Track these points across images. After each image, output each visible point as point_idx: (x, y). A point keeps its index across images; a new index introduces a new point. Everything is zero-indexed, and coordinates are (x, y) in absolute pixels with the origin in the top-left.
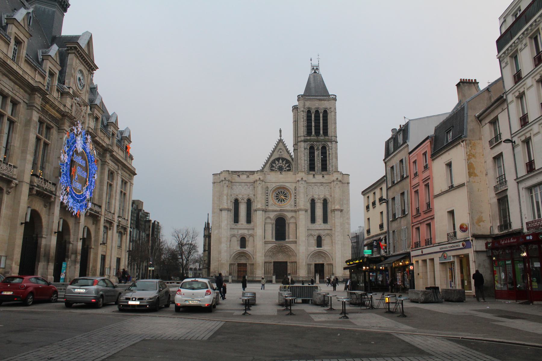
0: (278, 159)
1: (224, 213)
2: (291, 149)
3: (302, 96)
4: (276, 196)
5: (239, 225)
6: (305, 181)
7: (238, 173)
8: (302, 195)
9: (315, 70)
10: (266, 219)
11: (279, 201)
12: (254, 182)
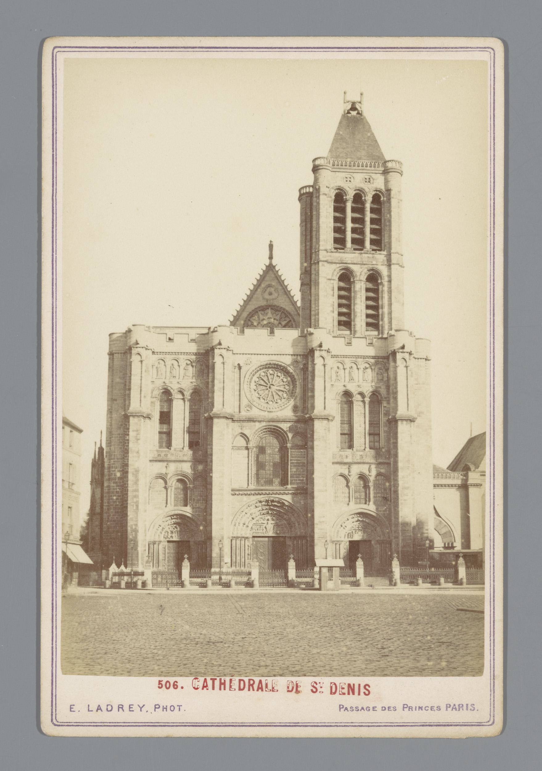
0: (263, 309)
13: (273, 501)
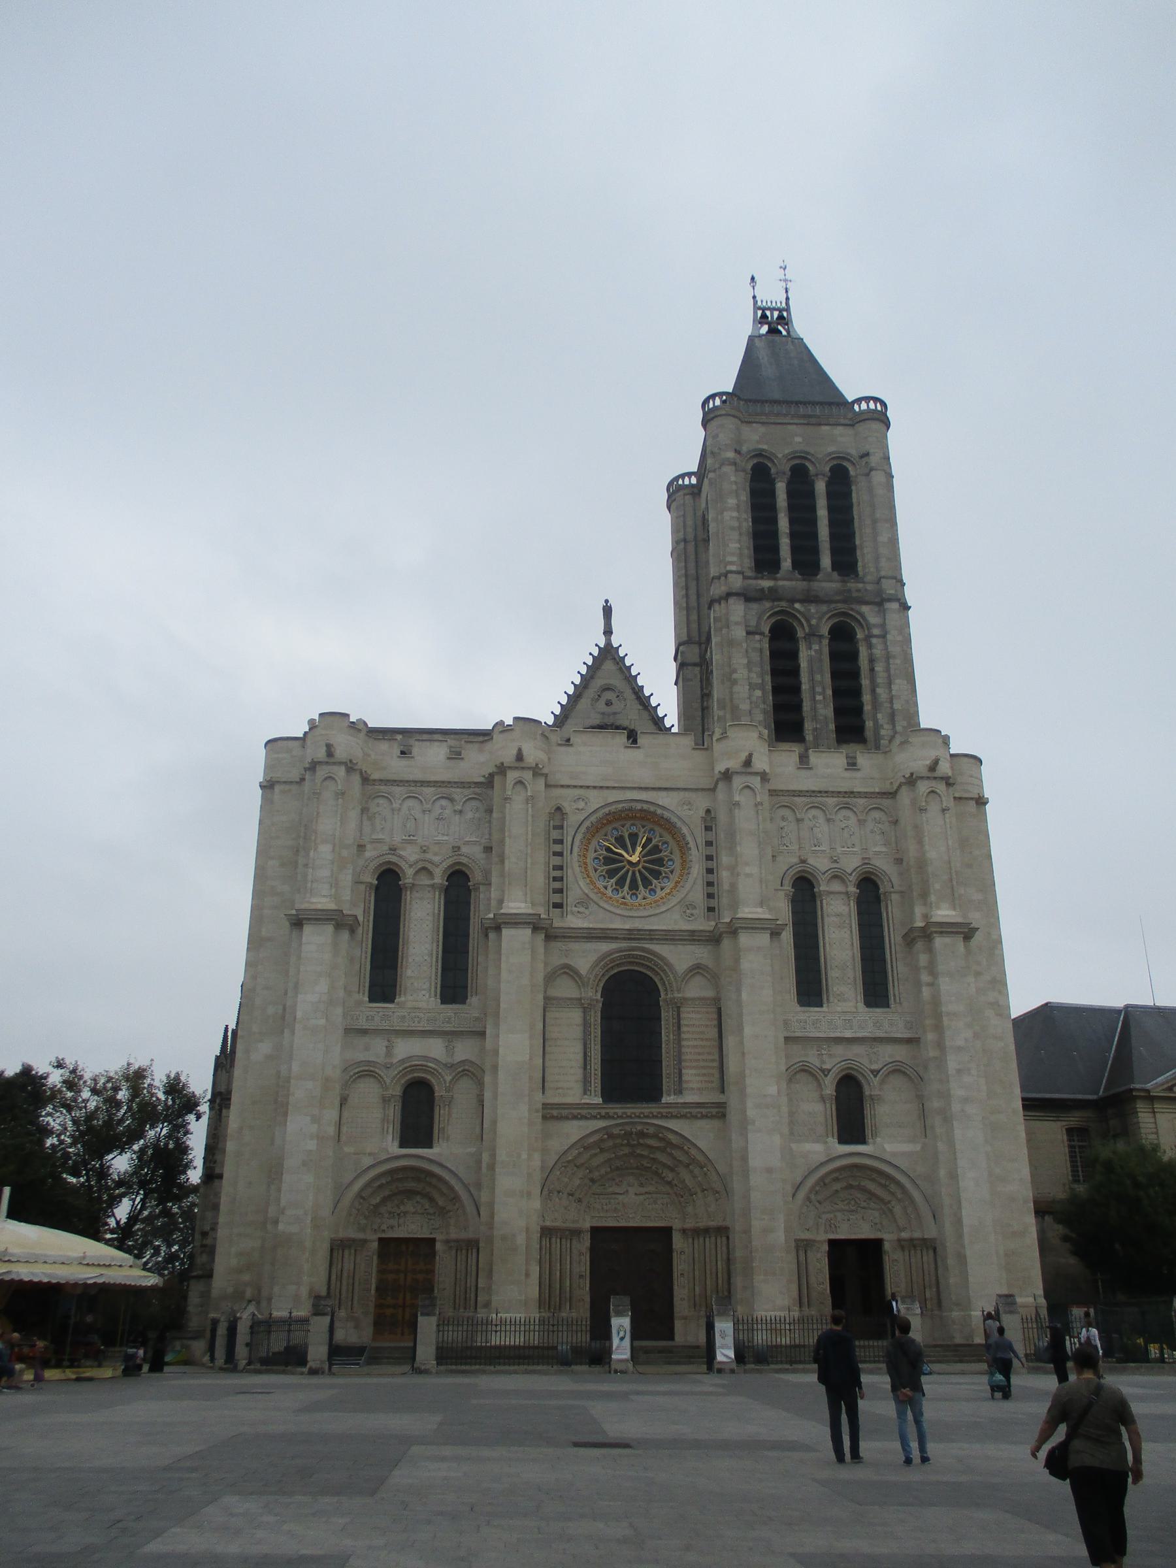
1: (317, 942)
4: (607, 861)
6: (764, 777)
8: (748, 848)
9: (774, 325)
10: (550, 978)
11: (620, 883)
12: (489, 782)
13: (642, 1134)
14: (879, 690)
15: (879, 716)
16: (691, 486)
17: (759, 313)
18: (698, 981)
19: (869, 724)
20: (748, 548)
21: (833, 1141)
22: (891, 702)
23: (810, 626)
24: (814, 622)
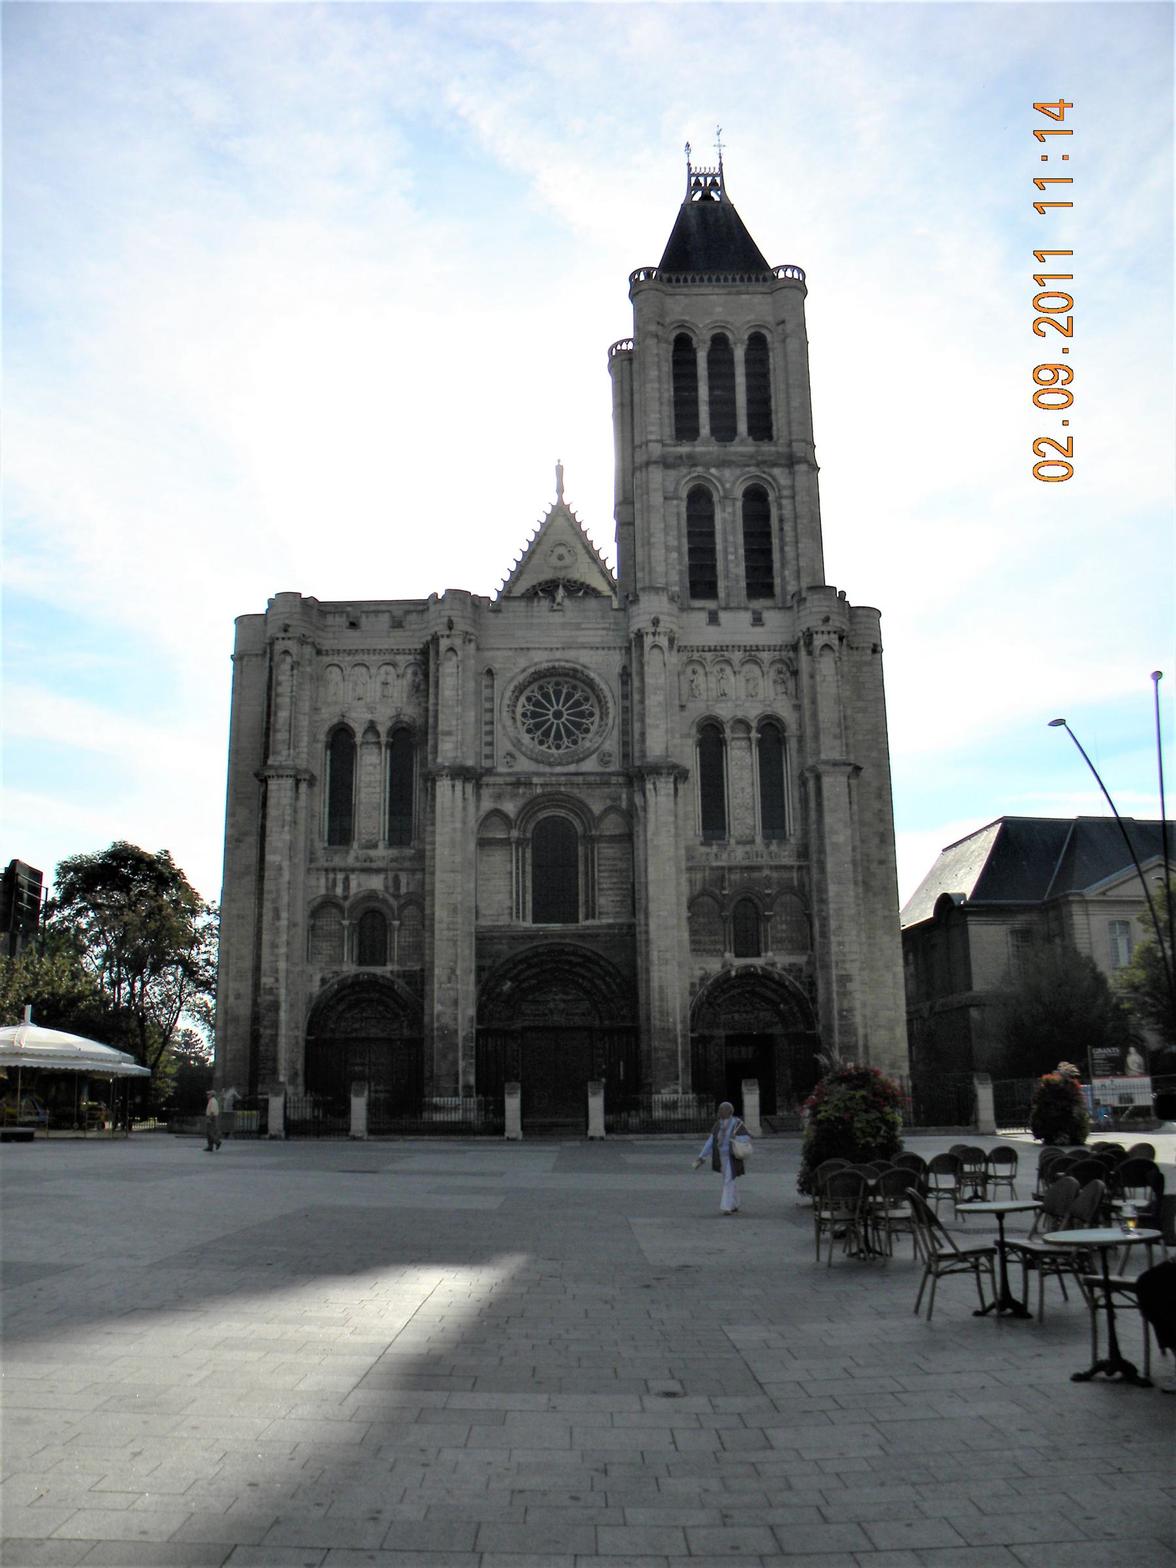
0: (548, 589)
2: (603, 535)
3: (648, 271)
5: (353, 855)
7: (353, 614)
14: (787, 549)
15: (787, 573)
16: (630, 352)
17: (693, 180)
18: (613, 817)
19: (777, 581)
20: (669, 417)
21: (728, 955)
22: (797, 559)
23: (724, 489)
24: (728, 486)
